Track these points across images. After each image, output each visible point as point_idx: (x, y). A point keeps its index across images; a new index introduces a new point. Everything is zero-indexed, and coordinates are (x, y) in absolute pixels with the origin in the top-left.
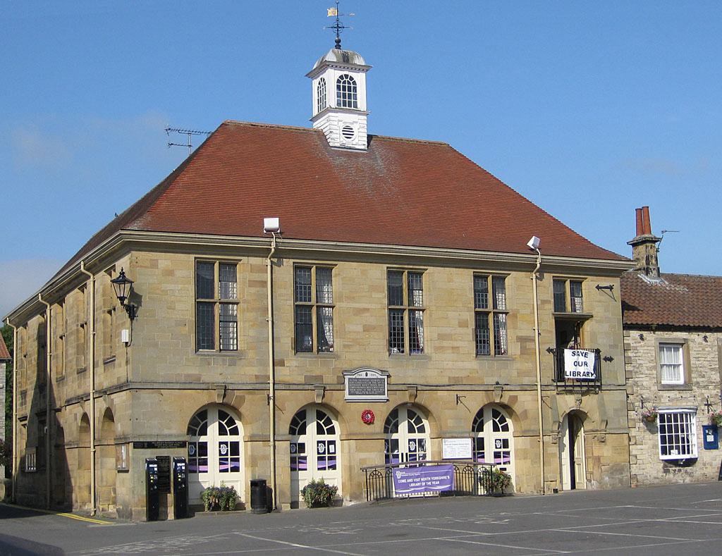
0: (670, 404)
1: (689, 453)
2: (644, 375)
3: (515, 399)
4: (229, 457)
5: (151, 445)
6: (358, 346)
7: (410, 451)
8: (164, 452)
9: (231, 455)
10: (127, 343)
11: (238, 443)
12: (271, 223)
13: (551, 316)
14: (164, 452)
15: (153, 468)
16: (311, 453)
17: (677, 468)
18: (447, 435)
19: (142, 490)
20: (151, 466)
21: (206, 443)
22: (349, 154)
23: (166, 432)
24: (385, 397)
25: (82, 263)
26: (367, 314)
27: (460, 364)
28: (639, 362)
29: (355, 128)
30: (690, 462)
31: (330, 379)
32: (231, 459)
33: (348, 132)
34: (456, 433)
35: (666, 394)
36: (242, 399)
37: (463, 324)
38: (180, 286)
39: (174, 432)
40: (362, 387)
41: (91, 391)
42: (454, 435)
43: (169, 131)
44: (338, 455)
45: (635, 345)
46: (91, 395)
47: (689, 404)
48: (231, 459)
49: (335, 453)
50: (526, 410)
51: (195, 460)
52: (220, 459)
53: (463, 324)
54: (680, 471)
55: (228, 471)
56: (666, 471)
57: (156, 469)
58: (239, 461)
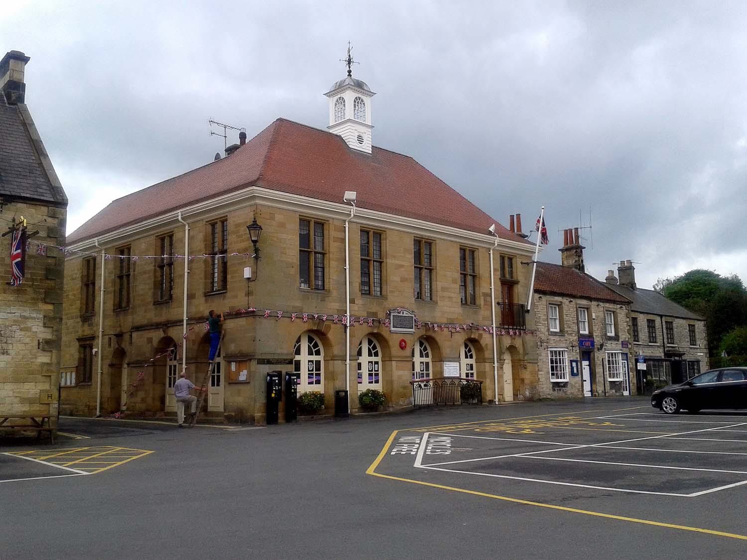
0: (554, 344)
1: (564, 378)
2: (540, 325)
3: (481, 335)
4: (314, 372)
5: (269, 362)
6: (398, 292)
7: (421, 371)
8: (278, 368)
9: (315, 371)
10: (248, 279)
11: (320, 361)
12: (350, 195)
13: (499, 280)
14: (278, 368)
15: (294, 379)
16: (365, 371)
17: (559, 388)
18: (447, 360)
19: (261, 400)
20: (273, 378)
21: (300, 361)
22: (361, 155)
23: (279, 351)
24: (413, 330)
25: (180, 214)
26: (403, 269)
27: (452, 309)
28: (539, 315)
29: (365, 137)
30: (565, 384)
31: (381, 315)
32: (316, 373)
33: (360, 139)
34: (452, 358)
35: (552, 338)
36: (329, 327)
37: (454, 282)
38: (290, 236)
39: (285, 351)
40: (402, 322)
41: (185, 318)
42: (451, 360)
43: (211, 123)
44: (380, 372)
45: (537, 304)
46: (185, 321)
47: (563, 345)
48: (316, 373)
49: (378, 371)
50: (486, 344)
51: (313, 373)
52: (309, 374)
53: (454, 282)
54: (560, 390)
55: (313, 384)
56: (554, 390)
57: (277, 381)
58: (320, 376)
